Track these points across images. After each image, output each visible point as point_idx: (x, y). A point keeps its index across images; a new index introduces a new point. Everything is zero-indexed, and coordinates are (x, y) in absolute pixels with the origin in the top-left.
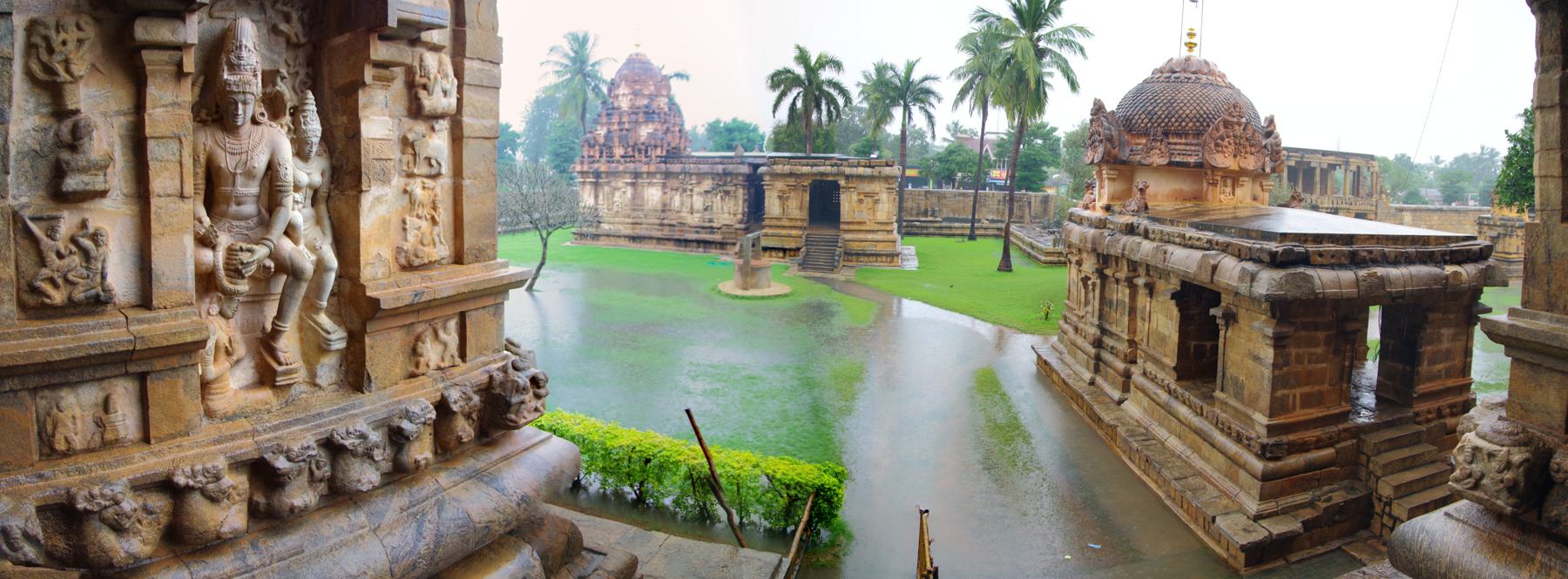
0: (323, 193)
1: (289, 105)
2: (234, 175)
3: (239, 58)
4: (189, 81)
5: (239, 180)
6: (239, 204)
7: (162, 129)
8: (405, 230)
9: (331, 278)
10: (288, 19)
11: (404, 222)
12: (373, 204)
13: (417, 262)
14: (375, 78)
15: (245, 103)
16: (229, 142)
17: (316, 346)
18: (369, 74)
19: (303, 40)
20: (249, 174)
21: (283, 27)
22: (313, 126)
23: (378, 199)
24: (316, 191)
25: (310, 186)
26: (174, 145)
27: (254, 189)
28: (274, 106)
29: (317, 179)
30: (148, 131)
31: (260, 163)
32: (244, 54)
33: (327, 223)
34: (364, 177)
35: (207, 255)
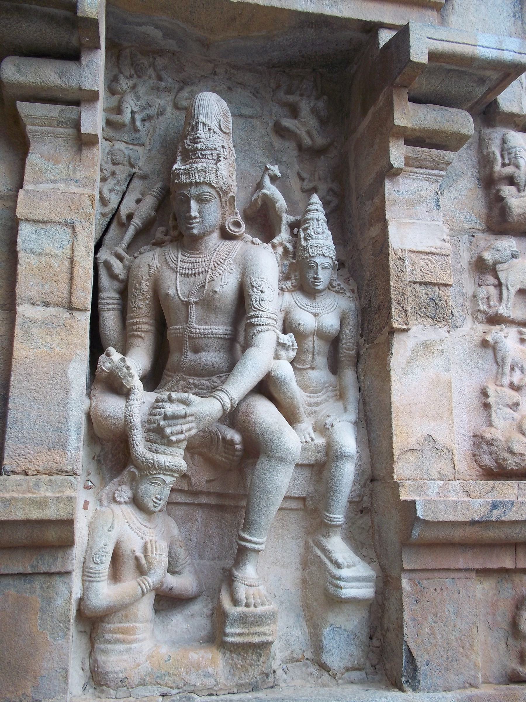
0: (347, 344)
1: (286, 218)
2: (187, 304)
3: (195, 140)
4: (99, 153)
5: (194, 312)
6: (196, 350)
7: (42, 211)
8: (487, 406)
9: (347, 473)
10: (294, 112)
11: (485, 393)
12: (415, 353)
13: (512, 463)
14: (409, 161)
15: (201, 200)
16: (181, 259)
17: (319, 595)
18: (398, 153)
19: (320, 141)
20: (208, 303)
21: (288, 123)
22: (322, 241)
23: (426, 347)
24: (334, 342)
25: (320, 333)
26: (65, 235)
27: (219, 328)
28: (262, 221)
29: (330, 321)
30: (21, 211)
31: (226, 285)
32: (202, 133)
33: (352, 394)
34: (395, 309)
35: (112, 406)
